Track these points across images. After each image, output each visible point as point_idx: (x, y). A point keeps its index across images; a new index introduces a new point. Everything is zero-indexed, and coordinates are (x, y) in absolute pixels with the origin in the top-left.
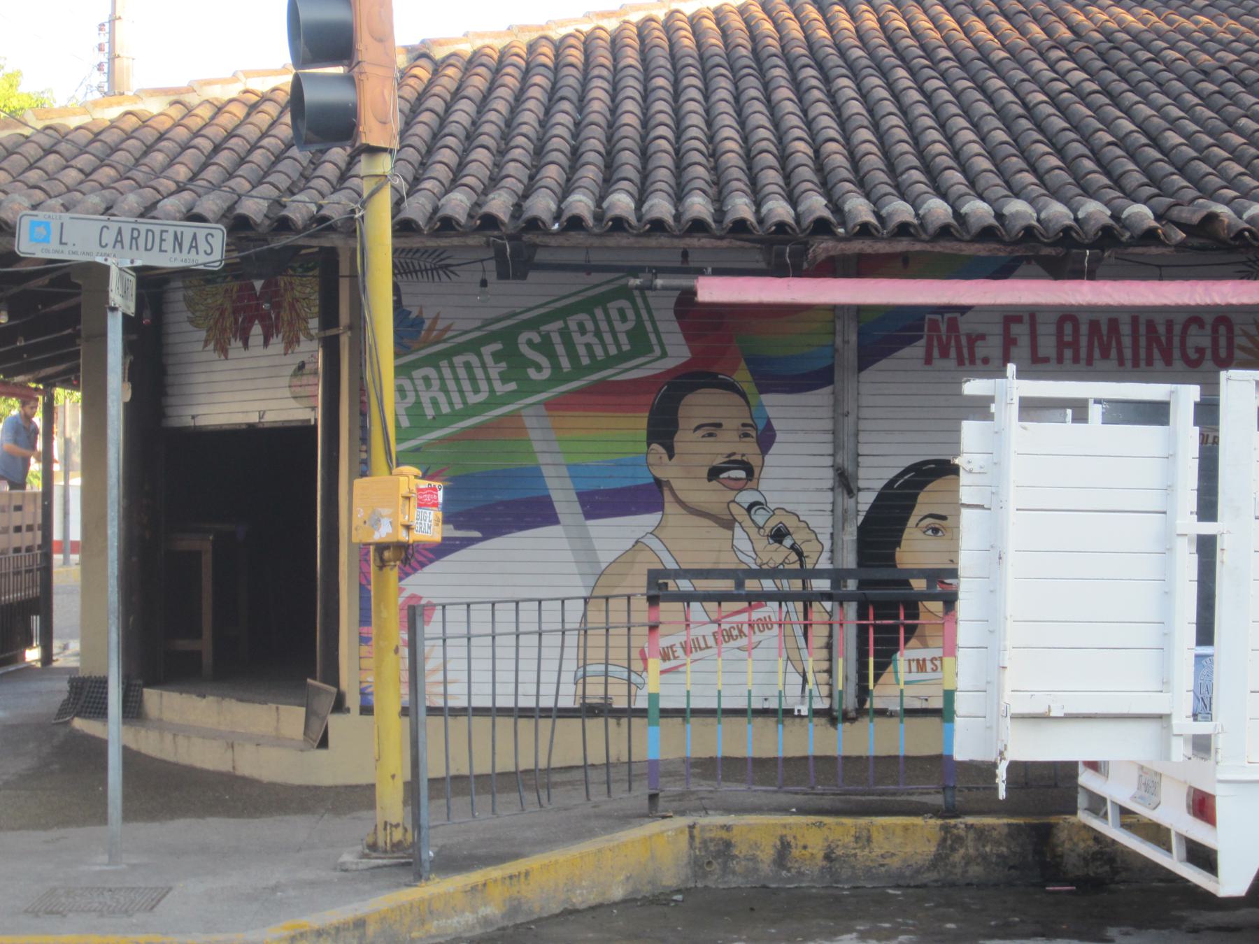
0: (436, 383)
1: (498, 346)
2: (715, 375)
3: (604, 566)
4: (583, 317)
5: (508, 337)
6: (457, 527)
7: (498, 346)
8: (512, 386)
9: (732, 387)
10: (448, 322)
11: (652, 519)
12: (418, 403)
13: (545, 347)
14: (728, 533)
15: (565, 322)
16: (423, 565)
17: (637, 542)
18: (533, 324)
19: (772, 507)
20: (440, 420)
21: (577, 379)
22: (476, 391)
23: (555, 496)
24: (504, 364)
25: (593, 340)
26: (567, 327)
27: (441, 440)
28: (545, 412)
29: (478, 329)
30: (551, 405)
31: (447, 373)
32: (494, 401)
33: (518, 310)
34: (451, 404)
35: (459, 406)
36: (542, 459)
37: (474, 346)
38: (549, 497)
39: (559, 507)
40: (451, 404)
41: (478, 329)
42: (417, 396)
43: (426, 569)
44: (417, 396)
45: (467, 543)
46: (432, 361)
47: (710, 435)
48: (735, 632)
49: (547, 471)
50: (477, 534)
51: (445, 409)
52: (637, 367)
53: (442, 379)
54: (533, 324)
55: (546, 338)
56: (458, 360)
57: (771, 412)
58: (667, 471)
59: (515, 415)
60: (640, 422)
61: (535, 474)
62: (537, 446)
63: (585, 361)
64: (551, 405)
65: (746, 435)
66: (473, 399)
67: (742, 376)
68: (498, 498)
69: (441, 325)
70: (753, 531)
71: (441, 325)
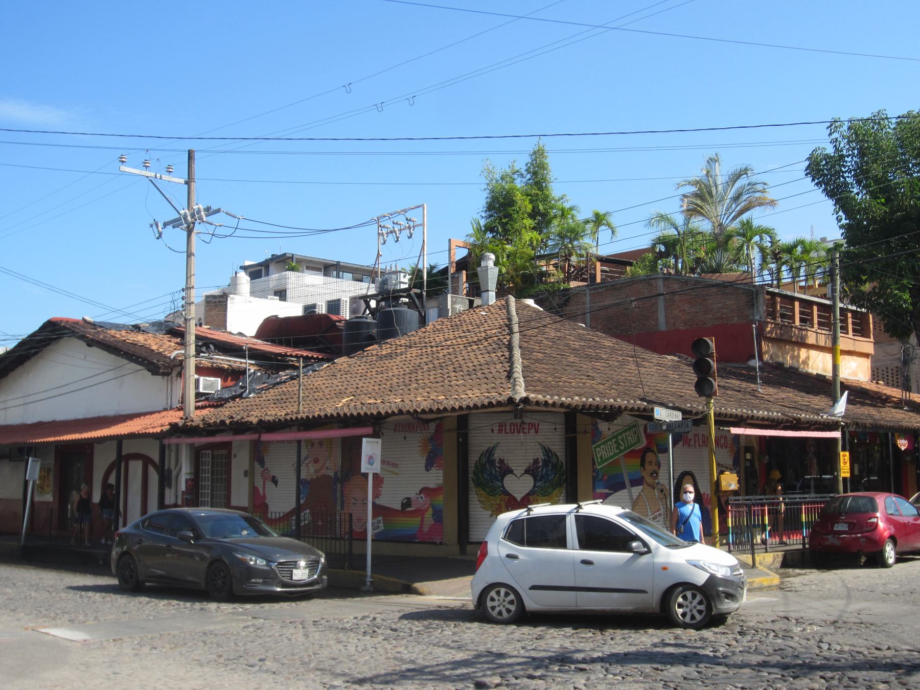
5: (616, 437)
9: (653, 452)
11: (641, 487)
13: (623, 440)
18: (621, 434)
20: (606, 460)
32: (615, 455)
37: (610, 440)
45: (611, 494)
46: (603, 443)
54: (621, 434)
58: (644, 474)
60: (638, 461)
61: (622, 475)
64: (624, 456)
67: (655, 449)
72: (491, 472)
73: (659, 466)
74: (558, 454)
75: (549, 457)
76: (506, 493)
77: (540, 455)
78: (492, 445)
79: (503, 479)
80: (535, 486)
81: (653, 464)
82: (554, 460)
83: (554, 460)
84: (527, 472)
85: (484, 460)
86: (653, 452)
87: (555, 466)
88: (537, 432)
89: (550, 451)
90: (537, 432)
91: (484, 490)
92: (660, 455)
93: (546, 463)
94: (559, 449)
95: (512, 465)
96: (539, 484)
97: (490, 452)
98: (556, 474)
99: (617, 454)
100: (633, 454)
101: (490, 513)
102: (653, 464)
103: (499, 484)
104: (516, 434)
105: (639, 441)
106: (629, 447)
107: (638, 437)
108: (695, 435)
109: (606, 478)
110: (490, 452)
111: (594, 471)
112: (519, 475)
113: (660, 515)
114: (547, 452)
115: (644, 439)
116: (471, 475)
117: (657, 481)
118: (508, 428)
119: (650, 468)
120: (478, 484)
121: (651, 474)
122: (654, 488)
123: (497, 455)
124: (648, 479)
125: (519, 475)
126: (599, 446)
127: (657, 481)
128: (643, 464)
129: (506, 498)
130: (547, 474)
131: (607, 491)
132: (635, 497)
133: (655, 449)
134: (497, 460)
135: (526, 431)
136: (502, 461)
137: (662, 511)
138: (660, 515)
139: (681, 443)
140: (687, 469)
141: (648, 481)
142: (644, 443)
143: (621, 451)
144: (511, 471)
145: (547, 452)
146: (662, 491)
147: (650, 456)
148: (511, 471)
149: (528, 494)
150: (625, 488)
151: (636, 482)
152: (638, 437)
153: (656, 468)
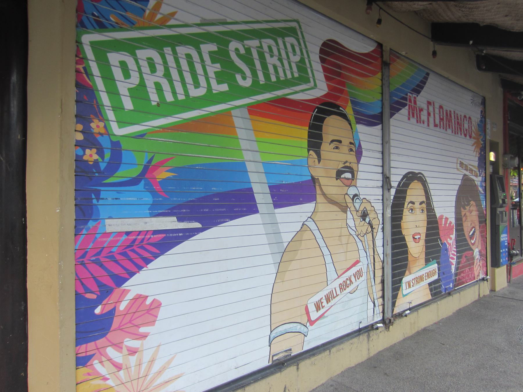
0: (160, 69)
1: (213, 47)
2: (338, 107)
3: (285, 245)
4: (271, 42)
5: (223, 40)
6: (180, 220)
7: (213, 47)
8: (224, 87)
9: (344, 116)
10: (171, 10)
11: (309, 207)
12: (142, 84)
14: (342, 215)
15: (260, 43)
16: (148, 261)
17: (303, 225)
19: (362, 197)
20: (163, 108)
21: (270, 92)
22: (197, 85)
23: (256, 188)
24: (218, 65)
25: (278, 64)
26: (261, 47)
27: (164, 129)
28: (247, 115)
29: (198, 25)
30: (254, 110)
31: (170, 59)
32: (210, 98)
33: (229, 20)
34: (174, 93)
35: (181, 97)
36: (247, 156)
37: (194, 41)
38: (251, 189)
39: (258, 198)
40: (174, 93)
41: (198, 25)
42: (142, 78)
43: (150, 266)
44: (142, 78)
45: (189, 234)
46: (157, 43)
47: (337, 148)
48: (348, 282)
49: (250, 167)
50: (197, 225)
51: (169, 98)
52: (302, 91)
53: (165, 62)
54: (240, 36)
55: (248, 50)
56: (182, 50)
57: (361, 137)
58: (318, 172)
59: (227, 114)
60: (304, 132)
61: (240, 168)
62: (244, 144)
63: (273, 79)
64: (254, 110)
65: (351, 150)
66: (194, 93)
67: (349, 111)
68: (215, 189)
69: (165, 10)
70: (354, 213)
71: (165, 10)
73: (359, 154)
81: (344, 149)
86: (344, 116)
92: (361, 128)
99: (222, 98)
100: (282, 109)
102: (344, 149)
105: (303, 77)
106: (270, 87)
107: (301, 66)
108: (429, 103)
109: (162, 175)
111: (90, 140)
113: (359, 274)
115: (320, 75)
117: (352, 191)
119: (333, 157)
121: (339, 174)
122: (344, 209)
124: (330, 186)
126: (130, 47)
127: (352, 191)
128: (315, 142)
131: (170, 223)
132: (287, 238)
133: (349, 111)
137: (363, 266)
138: (359, 274)
139: (404, 111)
140: (416, 168)
141: (328, 190)
142: (318, 88)
143: (236, 92)
146: (364, 215)
147: (333, 126)
150: (253, 209)
151: (286, 195)
152: (301, 66)
153: (351, 158)
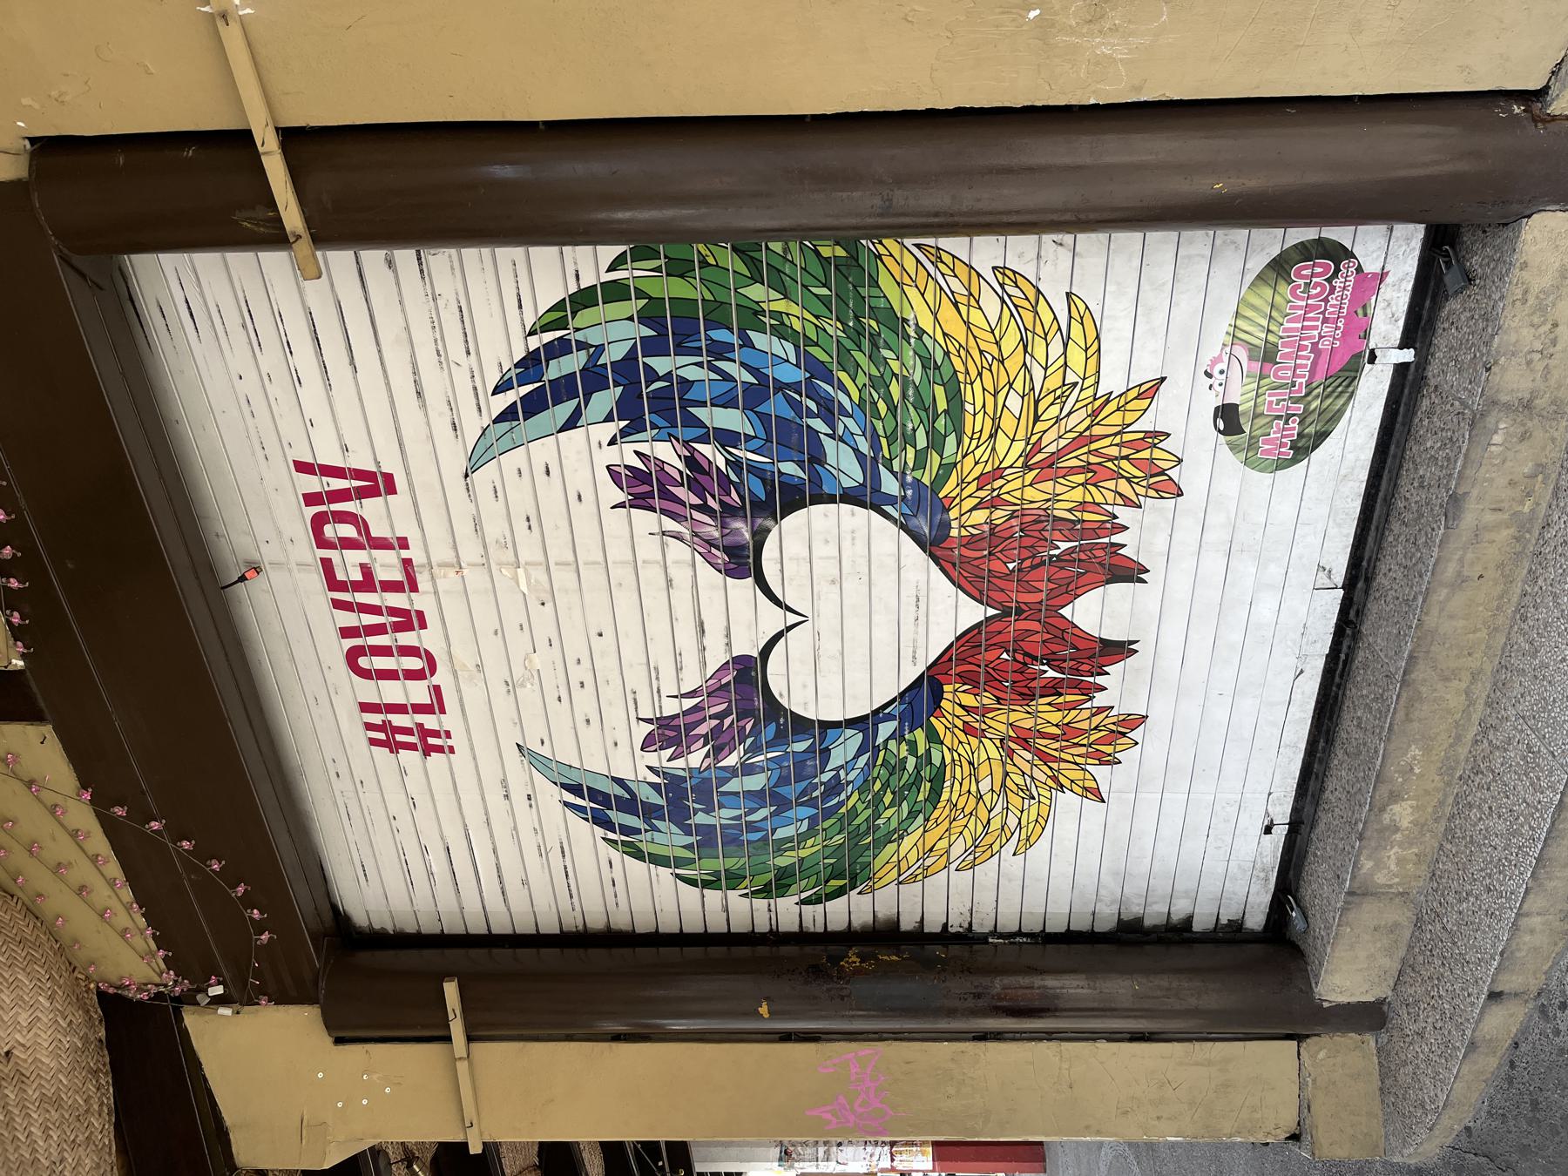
72: (758, 797)
74: (551, 292)
75: (594, 378)
76: (920, 699)
77: (589, 450)
78: (551, 796)
79: (802, 725)
80: (865, 497)
82: (616, 332)
83: (616, 332)
84: (742, 561)
85: (669, 839)
87: (670, 327)
88: (377, 484)
89: (531, 364)
90: (377, 484)
91: (900, 833)
93: (646, 404)
94: (501, 295)
95: (684, 672)
96: (844, 466)
97: (602, 804)
98: (753, 315)
101: (1067, 801)
103: (845, 748)
104: (428, 639)
110: (602, 804)
112: (773, 619)
114: (542, 389)
116: (787, 912)
118: (392, 692)
120: (850, 873)
123: (636, 766)
125: (773, 619)
129: (957, 697)
130: (753, 398)
134: (661, 758)
135: (386, 566)
136: (667, 733)
144: (746, 676)
145: (542, 389)
148: (746, 676)
149: (934, 545)
